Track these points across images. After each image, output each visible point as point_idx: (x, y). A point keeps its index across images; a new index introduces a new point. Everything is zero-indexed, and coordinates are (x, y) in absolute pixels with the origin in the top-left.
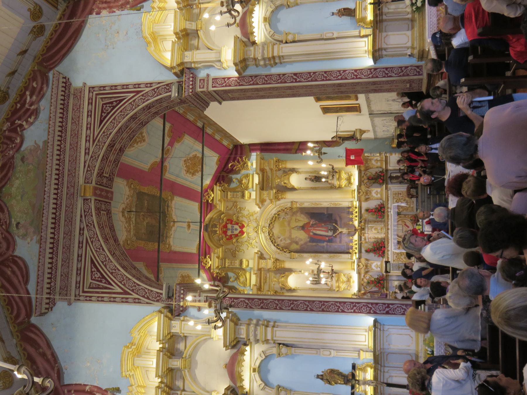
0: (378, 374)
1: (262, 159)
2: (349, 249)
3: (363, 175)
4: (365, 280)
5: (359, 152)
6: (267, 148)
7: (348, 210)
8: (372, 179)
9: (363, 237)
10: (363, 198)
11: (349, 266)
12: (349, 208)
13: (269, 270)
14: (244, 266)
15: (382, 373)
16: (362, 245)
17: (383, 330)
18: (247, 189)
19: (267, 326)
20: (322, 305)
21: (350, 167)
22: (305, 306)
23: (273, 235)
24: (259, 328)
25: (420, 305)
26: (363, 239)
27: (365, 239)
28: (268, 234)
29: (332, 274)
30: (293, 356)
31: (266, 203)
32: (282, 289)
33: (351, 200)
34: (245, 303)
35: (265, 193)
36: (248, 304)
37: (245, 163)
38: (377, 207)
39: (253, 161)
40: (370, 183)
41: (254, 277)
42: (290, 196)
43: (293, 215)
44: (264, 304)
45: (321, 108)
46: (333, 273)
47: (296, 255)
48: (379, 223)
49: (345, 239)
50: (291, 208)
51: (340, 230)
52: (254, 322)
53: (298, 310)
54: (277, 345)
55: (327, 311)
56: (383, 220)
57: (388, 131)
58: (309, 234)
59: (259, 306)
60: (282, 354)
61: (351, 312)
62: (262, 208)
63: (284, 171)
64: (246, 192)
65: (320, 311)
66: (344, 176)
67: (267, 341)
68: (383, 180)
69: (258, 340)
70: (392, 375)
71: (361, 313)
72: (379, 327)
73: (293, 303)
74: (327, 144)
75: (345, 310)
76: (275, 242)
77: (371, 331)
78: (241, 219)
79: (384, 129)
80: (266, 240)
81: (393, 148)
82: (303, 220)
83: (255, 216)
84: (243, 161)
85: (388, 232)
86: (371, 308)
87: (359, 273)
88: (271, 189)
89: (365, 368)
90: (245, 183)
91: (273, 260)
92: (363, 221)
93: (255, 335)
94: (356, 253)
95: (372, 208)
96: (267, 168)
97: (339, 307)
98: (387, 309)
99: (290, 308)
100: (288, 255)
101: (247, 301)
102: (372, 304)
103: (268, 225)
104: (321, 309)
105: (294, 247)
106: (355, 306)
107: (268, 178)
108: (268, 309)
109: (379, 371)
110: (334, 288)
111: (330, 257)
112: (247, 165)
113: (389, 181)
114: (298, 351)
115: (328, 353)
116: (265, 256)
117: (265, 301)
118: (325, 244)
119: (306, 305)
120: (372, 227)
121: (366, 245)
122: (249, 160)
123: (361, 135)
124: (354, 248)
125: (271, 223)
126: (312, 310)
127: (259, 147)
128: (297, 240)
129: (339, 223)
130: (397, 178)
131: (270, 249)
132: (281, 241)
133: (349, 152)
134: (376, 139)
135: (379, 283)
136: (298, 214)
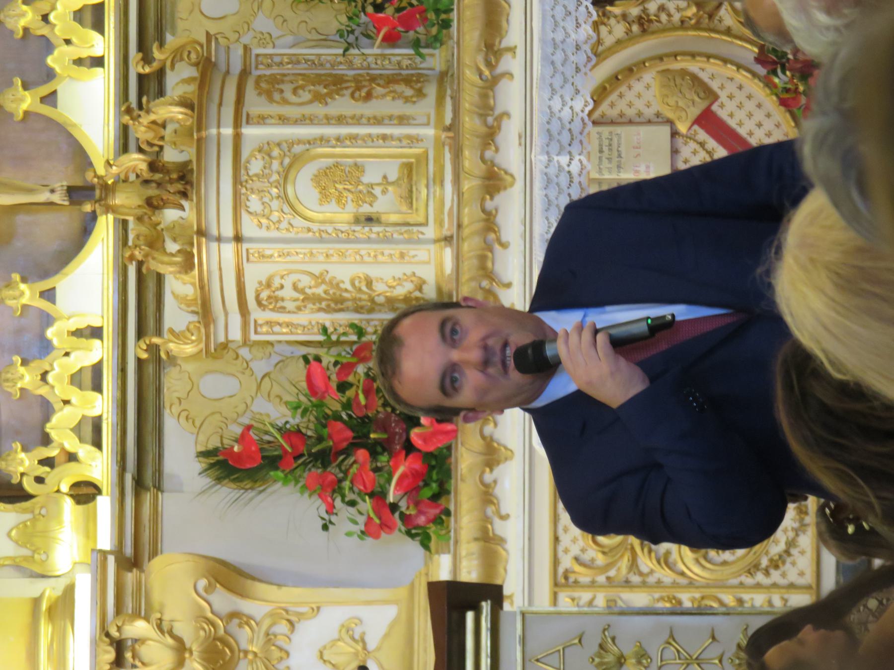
9: (178, 287)
16: (174, 384)
26: (176, 316)
27: (204, 310)
56: (436, 60)
85: (489, 223)
92: (179, 80)
120: (292, 158)
121: (220, 385)
124: (61, 427)
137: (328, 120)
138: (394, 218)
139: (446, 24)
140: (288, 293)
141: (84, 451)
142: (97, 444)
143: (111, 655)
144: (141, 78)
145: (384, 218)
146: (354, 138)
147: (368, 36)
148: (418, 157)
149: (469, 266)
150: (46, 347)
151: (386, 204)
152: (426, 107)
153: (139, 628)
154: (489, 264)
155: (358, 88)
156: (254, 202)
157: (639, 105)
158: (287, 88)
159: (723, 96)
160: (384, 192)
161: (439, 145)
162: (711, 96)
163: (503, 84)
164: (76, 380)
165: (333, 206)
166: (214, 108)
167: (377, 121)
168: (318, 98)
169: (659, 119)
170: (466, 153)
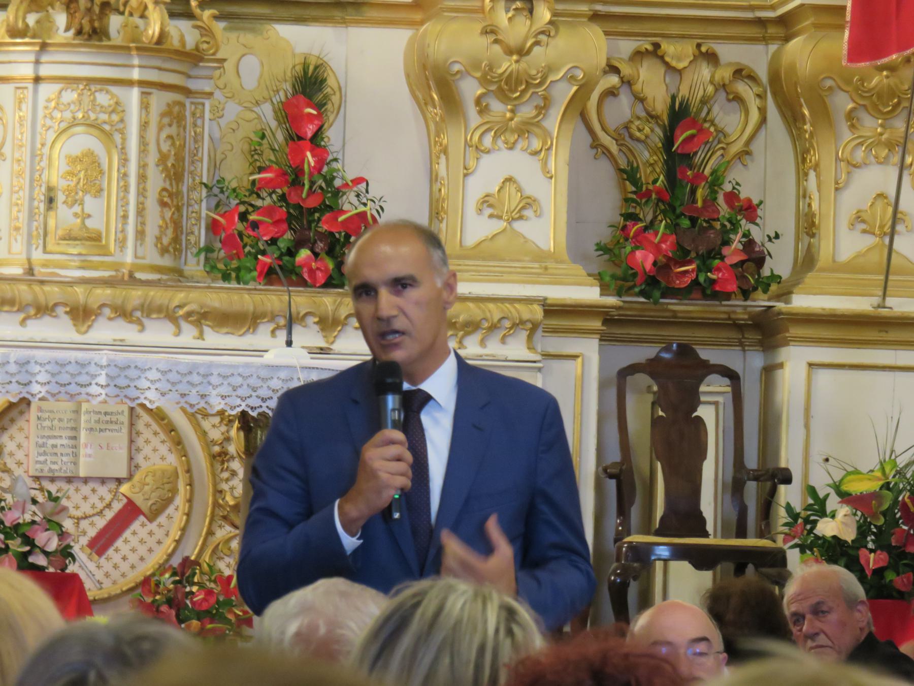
3: (732, 53)
8: (676, 161)
38: (350, 205)
40: (623, 134)
48: (154, 218)
56: (194, 266)
68: (654, 284)
85: (43, 310)
95: (332, 137)
113: (643, 353)
120: (108, 131)
130: (680, 441)
137: (143, 166)
138: (52, 223)
139: (226, 277)
145: (52, 214)
146: (126, 189)
147: (218, 205)
148: (106, 247)
149: (7, 290)
151: (64, 216)
152: (153, 257)
154: (6, 308)
155: (171, 195)
156: (70, 96)
157: (147, 450)
158: (173, 130)
159: (153, 526)
160: (76, 215)
161: (117, 266)
162: (153, 516)
163: (170, 327)
165: (64, 168)
166: (158, 63)
167: (140, 212)
168: (163, 159)
169: (133, 467)
170: (108, 291)
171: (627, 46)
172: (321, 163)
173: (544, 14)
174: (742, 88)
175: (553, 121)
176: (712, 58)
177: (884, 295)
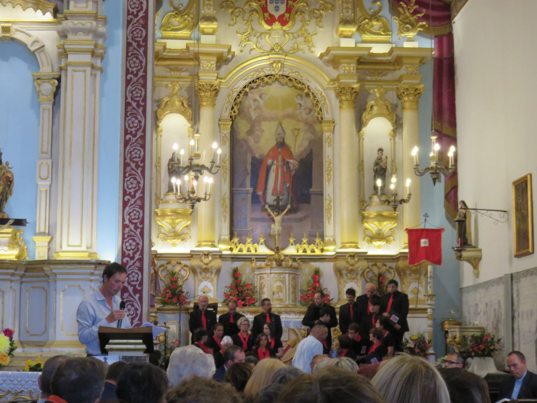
0: (7, 269)
1: (422, 61)
2: (239, 236)
3: (389, 264)
4: (177, 269)
5: (434, 255)
6: (445, 70)
7: (317, 234)
8: (380, 283)
9: (263, 264)
10: (341, 264)
11: (205, 235)
12: (322, 237)
13: (195, 76)
14: (203, 25)
15: (9, 277)
16: (248, 263)
17: (91, 281)
18: (358, 29)
19: (93, 54)
20: (137, 163)
21: (404, 238)
22: (133, 130)
23: (267, 83)
24: (90, 37)
25: (144, 343)
26: (259, 264)
28: (268, 73)
29: (190, 199)
30: (36, 105)
31: (330, 69)
32: (158, 103)
33: (339, 242)
34: (138, 12)
35: (352, 67)
36: (136, 16)
37: (413, 25)
39: (417, 42)
41: (180, 45)
42: (345, 117)
43: (306, 123)
44: (137, 46)
45: (526, 177)
46: (191, 199)
47: (227, 132)
48: (291, 296)
49: (259, 229)
50: (321, 121)
51: (278, 219)
52: (102, 29)
53: (126, 116)
54: (56, 74)
55: (125, 173)
56: (298, 304)
57: (477, 314)
58: (268, 155)
59: (133, 39)
60: (39, 85)
61: (124, 220)
62: (320, 62)
63: (396, 106)
64: (354, 29)
65: (125, 159)
66: (387, 226)
67: (64, 53)
69: (66, 37)
70: (6, 297)
71: (123, 238)
72: (96, 272)
73: (139, 106)
74: (452, 192)
75: (127, 209)
76: (252, 88)
77: (89, 256)
78: (298, 17)
79: (481, 307)
80: (256, 70)
81: (442, 324)
82: (298, 145)
83: (304, 47)
84: (418, 22)
86: (132, 258)
87: (192, 255)
88: (360, 80)
89: (17, 243)
90: (372, 26)
91: (216, 82)
93: (75, 31)
94: (231, 249)
96: (402, 71)
97: (133, 197)
98: (131, 289)
99: (129, 100)
100: (226, 115)
101: (141, 14)
102: (141, 260)
103: (286, 73)
104: (128, 161)
105: (243, 127)
106: (136, 228)
107: (380, 73)
108: (127, 56)
109: (13, 271)
110: (160, 207)
111: (224, 200)
112: (408, 30)
114: (47, 115)
115: (44, 174)
116: (224, 68)
117: (142, 50)
118: (250, 189)
119: (137, 131)
120: (283, 282)
121: (248, 271)
122: (420, 34)
123: (469, 260)
124: (241, 246)
125: (290, 80)
126: (126, 143)
127: (445, 55)
128: (257, 132)
129: (291, 216)
131: (236, 79)
132: (255, 100)
133: (435, 235)
134: (461, 290)
135: (174, 294)
136: (309, 135)
137: (289, 288)
140: (262, 281)
141: (238, 249)
142: (239, 251)
143: (206, 253)
144: (295, 259)
150: (254, 243)
152: (291, 302)
153: (210, 258)
156: (276, 276)
164: (249, 248)
167: (289, 295)
168: (292, 286)
169: (289, 339)
171: (371, 264)
172: (319, 286)
173: (356, 259)
174: (391, 271)
175: (359, 277)
176: (385, 265)
177: (417, 303)
